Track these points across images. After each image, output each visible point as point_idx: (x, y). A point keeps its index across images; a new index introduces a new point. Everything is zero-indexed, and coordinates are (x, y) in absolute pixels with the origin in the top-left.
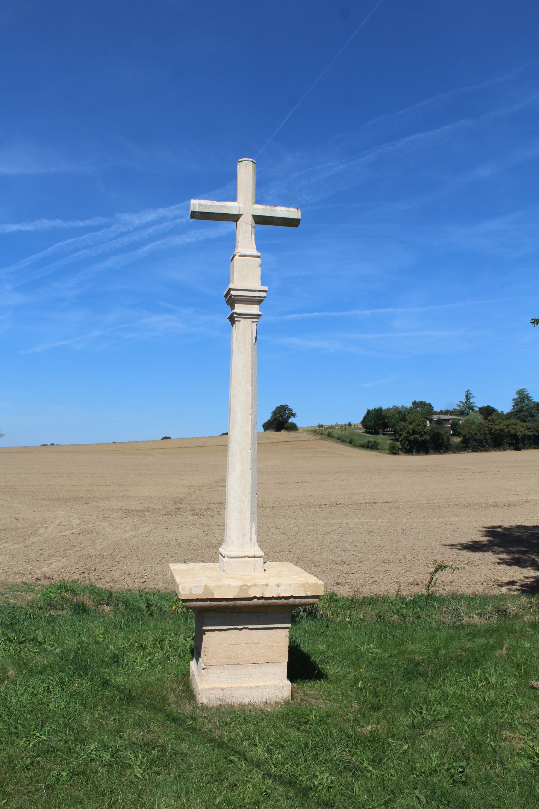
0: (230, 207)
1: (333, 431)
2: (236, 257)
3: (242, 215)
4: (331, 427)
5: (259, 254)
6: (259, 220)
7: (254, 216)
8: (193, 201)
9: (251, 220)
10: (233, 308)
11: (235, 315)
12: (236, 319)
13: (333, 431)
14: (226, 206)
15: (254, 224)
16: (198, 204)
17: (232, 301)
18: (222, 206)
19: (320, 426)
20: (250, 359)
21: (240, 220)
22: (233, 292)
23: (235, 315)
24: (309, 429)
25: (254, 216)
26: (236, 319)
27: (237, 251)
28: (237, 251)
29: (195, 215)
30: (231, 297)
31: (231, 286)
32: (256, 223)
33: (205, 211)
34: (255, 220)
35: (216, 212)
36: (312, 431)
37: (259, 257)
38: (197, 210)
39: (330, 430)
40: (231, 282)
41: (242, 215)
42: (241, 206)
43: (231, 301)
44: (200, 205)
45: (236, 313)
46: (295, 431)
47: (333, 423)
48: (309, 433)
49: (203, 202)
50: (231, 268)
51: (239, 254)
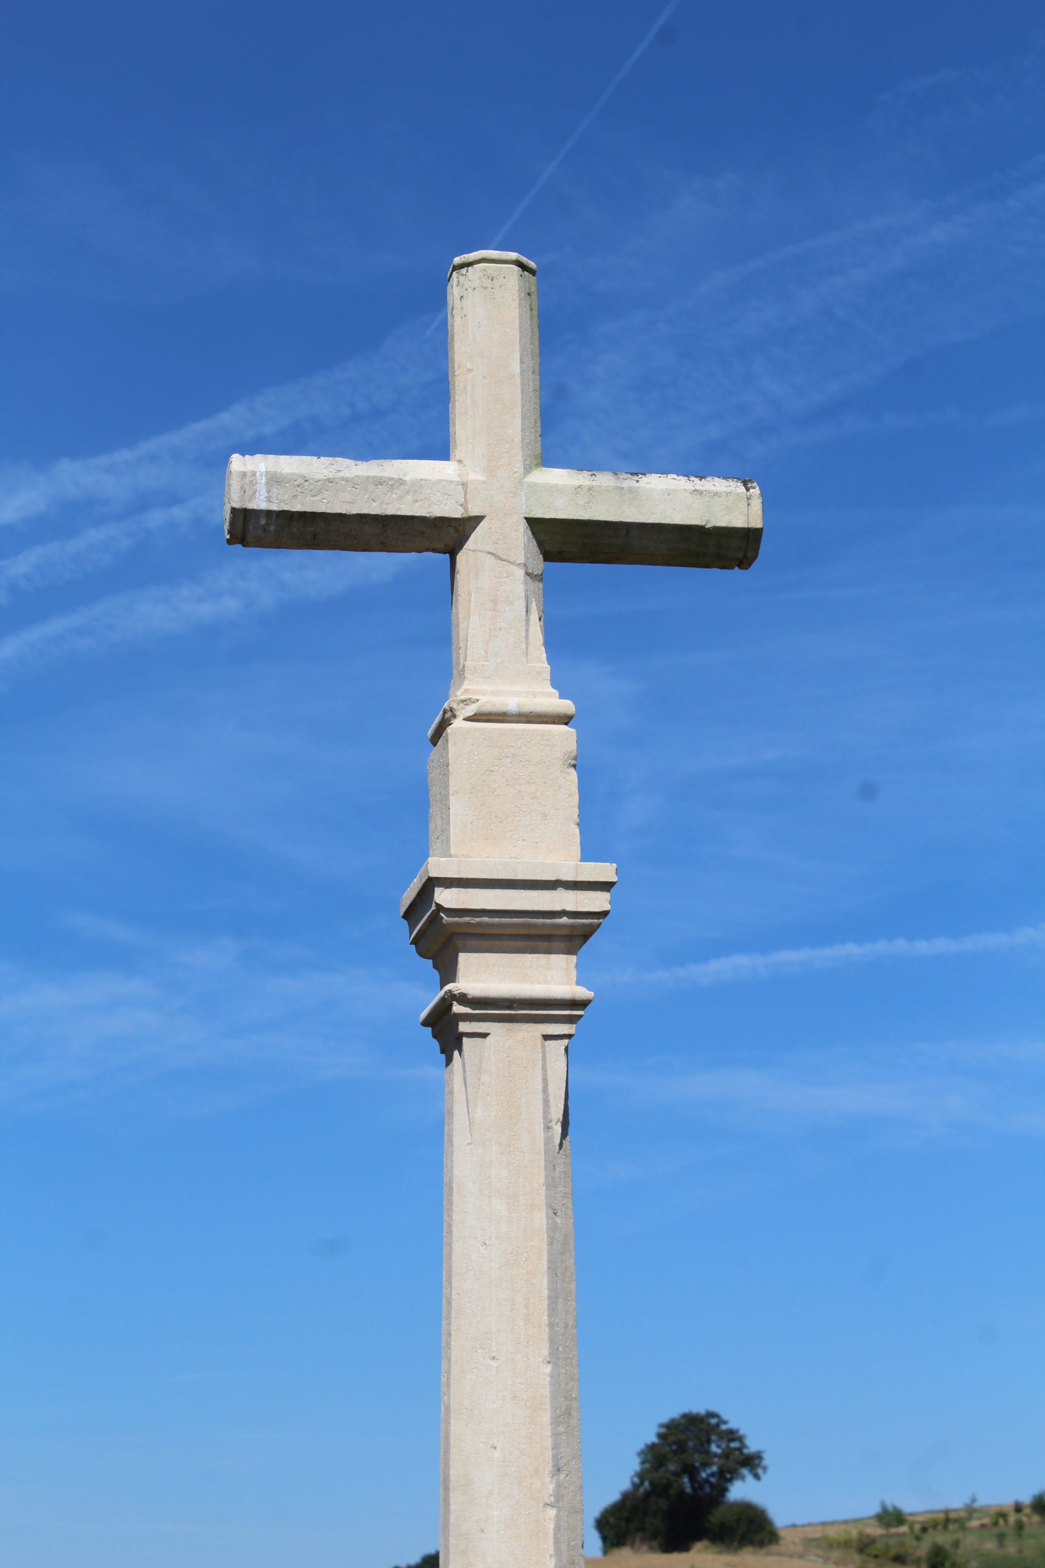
0: (419, 485)
1: (956, 1544)
2: (458, 724)
3: (478, 520)
4: (947, 1521)
5: (567, 706)
6: (563, 542)
7: (533, 523)
8: (238, 463)
9: (520, 545)
10: (448, 972)
11: (457, 1008)
12: (464, 1027)
13: (956, 1544)
14: (401, 482)
15: (538, 564)
16: (262, 478)
17: (440, 938)
18: (379, 482)
19: (891, 1517)
20: (540, 1219)
21: (470, 544)
22: (444, 897)
23: (457, 1008)
24: (832, 1532)
25: (533, 523)
26: (464, 1027)
27: (460, 694)
28: (460, 694)
29: (252, 529)
30: (435, 918)
31: (437, 866)
32: (548, 556)
33: (298, 507)
34: (540, 544)
35: (354, 510)
36: (846, 1544)
37: (565, 720)
38: (260, 503)
39: (943, 1539)
40: (436, 846)
41: (478, 520)
42: (475, 476)
43: (440, 938)
44: (275, 480)
45: (463, 999)
46: (761, 1544)
47: (956, 1501)
48: (836, 1554)
49: (288, 465)
50: (434, 774)
51: (470, 710)
